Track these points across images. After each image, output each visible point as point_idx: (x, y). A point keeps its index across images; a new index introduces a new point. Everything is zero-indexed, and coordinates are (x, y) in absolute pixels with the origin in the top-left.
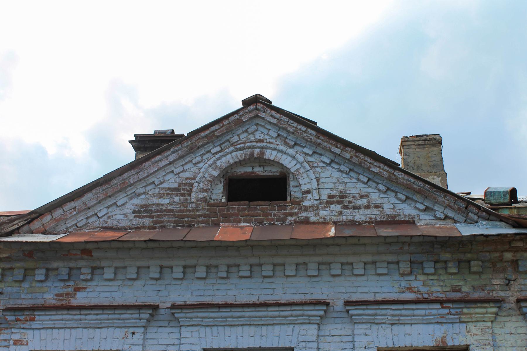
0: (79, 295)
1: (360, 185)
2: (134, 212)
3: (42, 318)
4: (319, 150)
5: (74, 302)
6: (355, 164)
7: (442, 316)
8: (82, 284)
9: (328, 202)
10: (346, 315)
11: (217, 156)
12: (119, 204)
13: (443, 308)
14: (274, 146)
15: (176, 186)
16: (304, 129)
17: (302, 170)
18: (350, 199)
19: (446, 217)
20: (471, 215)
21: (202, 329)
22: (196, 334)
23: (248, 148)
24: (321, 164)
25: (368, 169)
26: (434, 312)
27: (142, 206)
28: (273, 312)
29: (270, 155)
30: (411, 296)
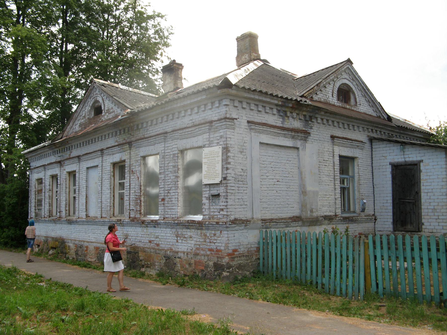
5: (71, 156)
13: (119, 147)
23: (95, 97)
26: (117, 149)
30: (116, 144)
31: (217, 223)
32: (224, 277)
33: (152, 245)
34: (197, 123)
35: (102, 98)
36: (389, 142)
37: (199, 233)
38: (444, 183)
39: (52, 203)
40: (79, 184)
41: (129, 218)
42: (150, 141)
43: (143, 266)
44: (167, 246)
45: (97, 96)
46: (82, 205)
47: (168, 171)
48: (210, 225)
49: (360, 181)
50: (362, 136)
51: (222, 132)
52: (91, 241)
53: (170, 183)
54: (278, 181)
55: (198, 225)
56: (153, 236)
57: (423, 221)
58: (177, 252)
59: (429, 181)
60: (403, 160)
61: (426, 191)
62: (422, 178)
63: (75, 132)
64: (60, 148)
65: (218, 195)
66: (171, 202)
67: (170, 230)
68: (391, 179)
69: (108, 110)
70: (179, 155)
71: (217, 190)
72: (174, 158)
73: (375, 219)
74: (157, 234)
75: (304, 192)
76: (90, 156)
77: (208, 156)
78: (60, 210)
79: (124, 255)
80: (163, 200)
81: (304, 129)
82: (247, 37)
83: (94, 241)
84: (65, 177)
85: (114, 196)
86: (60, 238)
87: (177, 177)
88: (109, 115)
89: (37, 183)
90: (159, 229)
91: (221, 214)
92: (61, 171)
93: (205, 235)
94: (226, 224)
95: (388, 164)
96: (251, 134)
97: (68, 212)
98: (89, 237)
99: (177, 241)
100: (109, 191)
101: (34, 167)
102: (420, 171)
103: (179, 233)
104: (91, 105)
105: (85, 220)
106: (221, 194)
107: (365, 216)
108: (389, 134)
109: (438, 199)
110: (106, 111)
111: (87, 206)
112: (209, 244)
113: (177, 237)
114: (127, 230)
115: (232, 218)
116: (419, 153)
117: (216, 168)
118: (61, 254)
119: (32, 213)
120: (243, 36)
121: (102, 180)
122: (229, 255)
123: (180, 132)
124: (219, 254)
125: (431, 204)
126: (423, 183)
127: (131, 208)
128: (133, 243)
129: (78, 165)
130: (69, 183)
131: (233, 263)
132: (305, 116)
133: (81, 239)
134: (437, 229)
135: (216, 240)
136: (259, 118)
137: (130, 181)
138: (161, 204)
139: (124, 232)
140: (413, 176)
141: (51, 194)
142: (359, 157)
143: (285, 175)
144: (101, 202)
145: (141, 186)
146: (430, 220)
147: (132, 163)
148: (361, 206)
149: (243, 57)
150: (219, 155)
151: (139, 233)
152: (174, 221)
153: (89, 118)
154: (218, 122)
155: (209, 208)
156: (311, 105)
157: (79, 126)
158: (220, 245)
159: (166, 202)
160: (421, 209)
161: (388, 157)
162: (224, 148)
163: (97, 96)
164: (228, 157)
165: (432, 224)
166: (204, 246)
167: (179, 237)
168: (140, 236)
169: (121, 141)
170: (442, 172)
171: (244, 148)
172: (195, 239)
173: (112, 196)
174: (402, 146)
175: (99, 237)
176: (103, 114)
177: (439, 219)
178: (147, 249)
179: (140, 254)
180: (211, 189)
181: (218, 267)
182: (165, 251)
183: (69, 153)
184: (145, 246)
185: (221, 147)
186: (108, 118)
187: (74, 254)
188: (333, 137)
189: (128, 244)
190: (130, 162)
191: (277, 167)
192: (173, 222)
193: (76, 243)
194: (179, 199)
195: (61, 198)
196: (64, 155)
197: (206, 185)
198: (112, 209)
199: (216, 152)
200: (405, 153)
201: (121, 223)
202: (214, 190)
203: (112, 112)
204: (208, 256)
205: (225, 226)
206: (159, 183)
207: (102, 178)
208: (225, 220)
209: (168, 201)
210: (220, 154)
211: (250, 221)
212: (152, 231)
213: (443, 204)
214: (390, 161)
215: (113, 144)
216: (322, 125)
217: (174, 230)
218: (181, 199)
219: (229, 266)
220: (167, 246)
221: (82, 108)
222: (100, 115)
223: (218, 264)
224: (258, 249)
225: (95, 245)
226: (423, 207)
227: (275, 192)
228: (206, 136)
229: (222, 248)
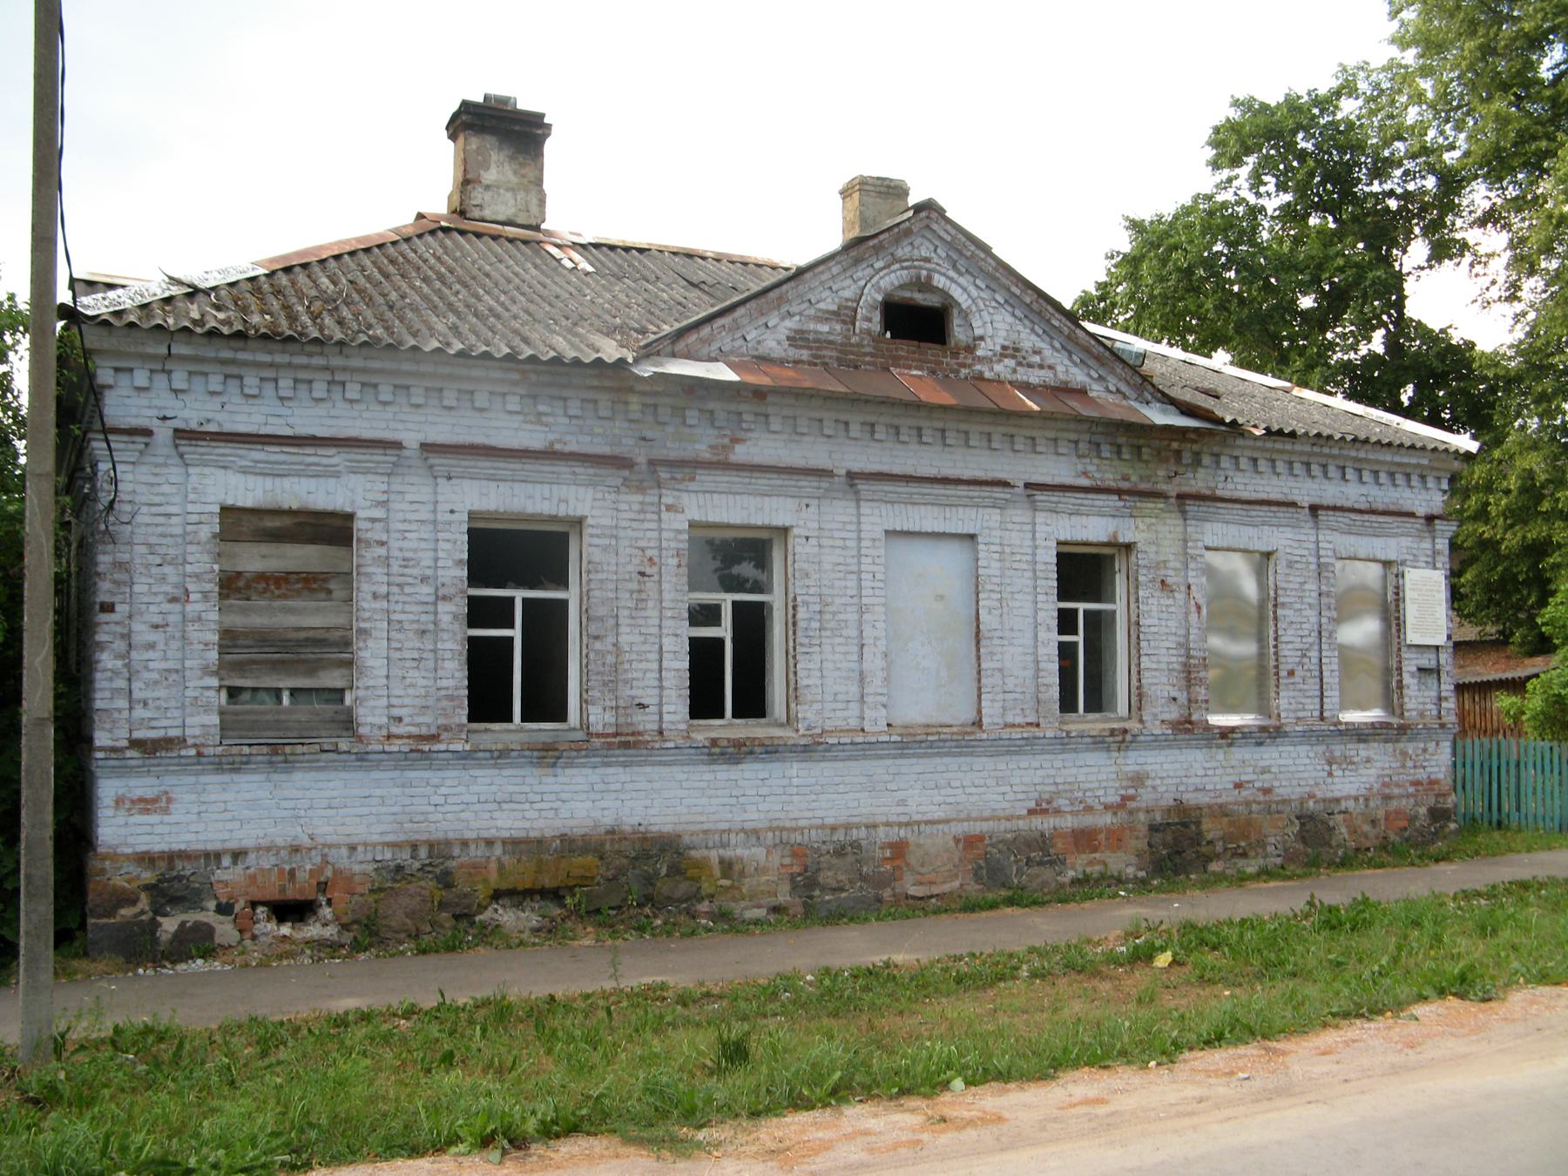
0: (739, 448)
1: (1033, 337)
2: (788, 338)
3: (703, 478)
4: (993, 285)
5: (733, 458)
6: (1032, 310)
7: (1117, 509)
8: (741, 435)
9: (1001, 355)
10: (1025, 499)
11: (881, 274)
12: (770, 325)
13: (1120, 499)
14: (943, 271)
15: (835, 308)
16: (983, 256)
17: (974, 309)
18: (1024, 353)
19: (1118, 391)
20: (1146, 394)
21: (883, 506)
22: (876, 512)
23: (915, 267)
24: (994, 304)
25: (1048, 321)
26: (1111, 503)
27: (796, 331)
28: (962, 491)
29: (939, 281)
30: (1085, 482)
32: (1451, 832)
33: (1245, 793)
34: (1381, 507)
42: (1254, 513)
47: (1302, 603)
56: (1251, 769)
58: (1337, 800)
74: (1261, 763)
79: (1137, 838)
80: (1291, 673)
83: (939, 814)
86: (612, 832)
90: (1274, 748)
93: (1404, 754)
98: (902, 802)
99: (1330, 774)
103: (1337, 754)
113: (1330, 763)
114: (1141, 760)
117: (1438, 616)
123: (1353, 516)
139: (1128, 768)
151: (1196, 765)
158: (1436, 769)
168: (1200, 772)
169: (1110, 478)
172: (1378, 765)
175: (972, 799)
179: (1206, 825)
181: (1439, 815)
187: (786, 887)
212: (1247, 756)
215: (1069, 480)
217: (1321, 749)
220: (1299, 790)
225: (959, 829)
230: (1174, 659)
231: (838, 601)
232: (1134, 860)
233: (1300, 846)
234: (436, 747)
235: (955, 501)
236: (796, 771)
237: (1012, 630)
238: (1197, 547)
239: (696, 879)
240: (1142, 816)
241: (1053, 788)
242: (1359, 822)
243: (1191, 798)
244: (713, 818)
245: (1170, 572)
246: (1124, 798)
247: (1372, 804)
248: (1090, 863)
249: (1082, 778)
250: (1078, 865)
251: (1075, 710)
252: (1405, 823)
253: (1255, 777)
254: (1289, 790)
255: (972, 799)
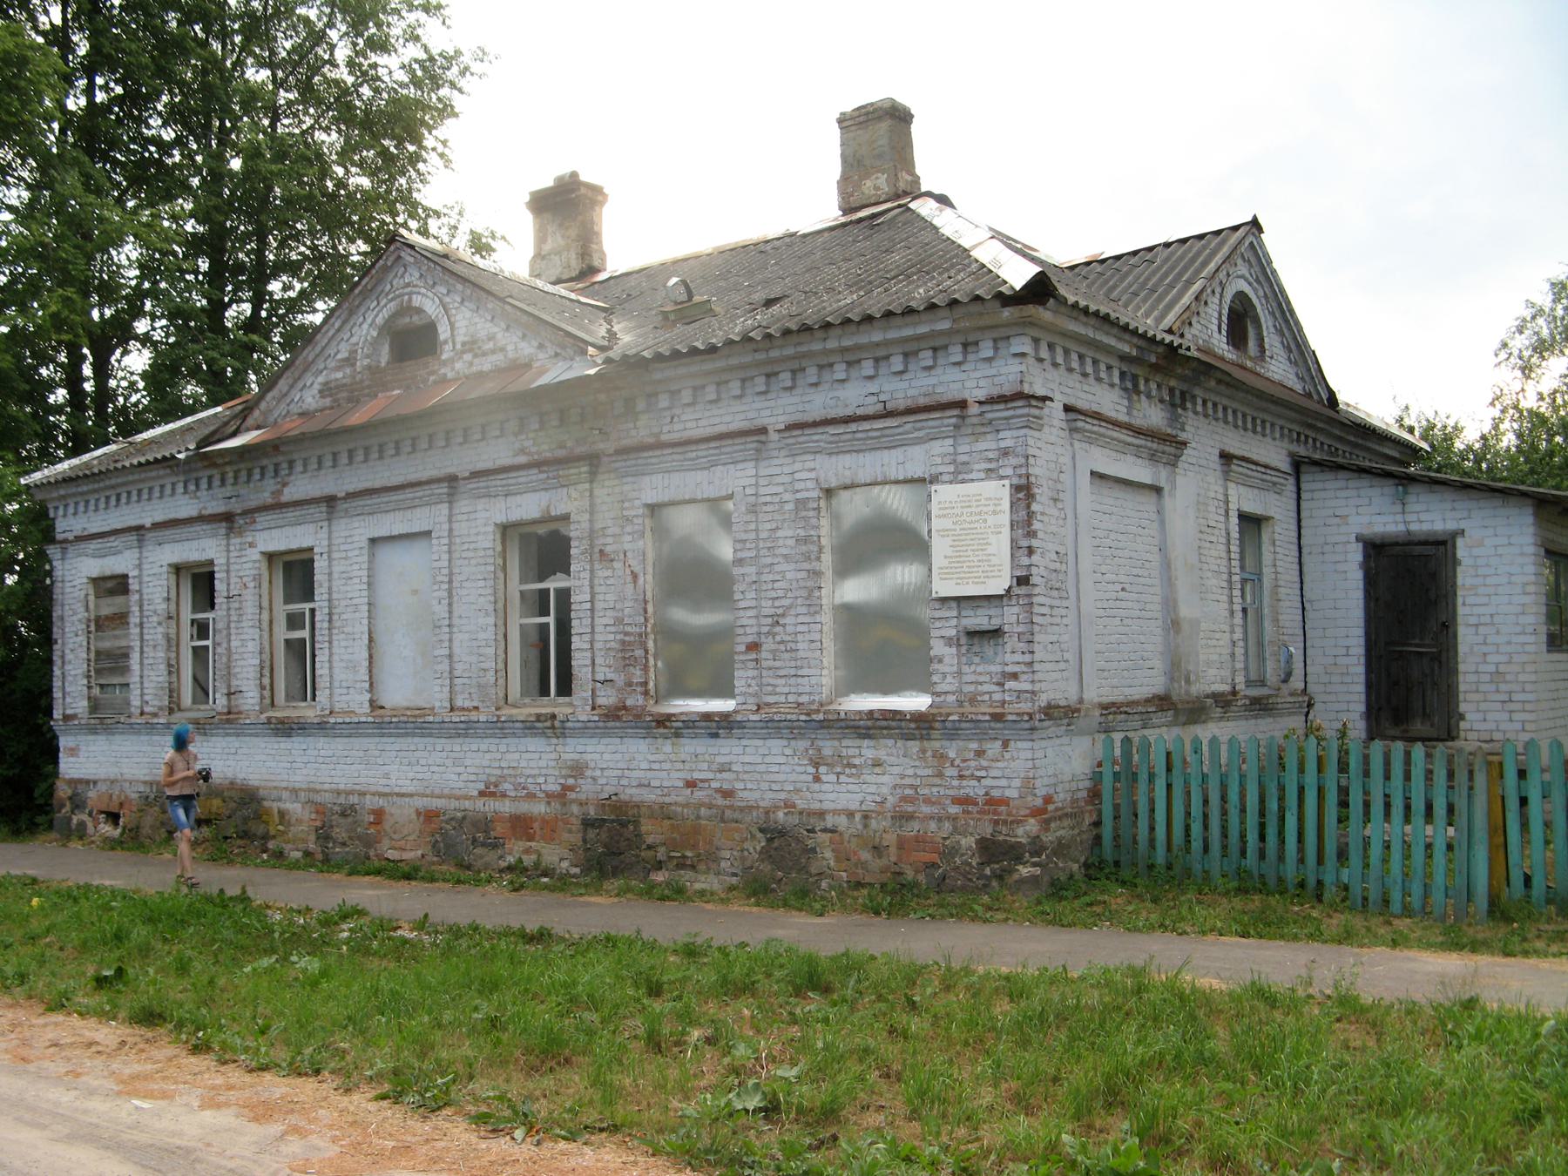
0: (286, 490)
13: (541, 472)
23: (398, 296)
26: (534, 478)
30: (522, 459)
31: (998, 717)
33: (699, 794)
34: (902, 404)
35: (441, 301)
36: (1356, 475)
37: (915, 750)
38: (1527, 599)
39: (178, 663)
40: (330, 594)
41: (593, 708)
43: (659, 865)
44: (771, 795)
45: (410, 294)
46: (354, 668)
47: (775, 555)
48: (964, 725)
49: (1280, 589)
50: (1274, 453)
51: (1008, 439)
52: (397, 790)
53: (780, 593)
54: (1123, 589)
55: (913, 725)
56: (705, 766)
57: (1463, 707)
58: (821, 814)
59: (1481, 590)
60: (1401, 528)
61: (1473, 620)
62: (1460, 581)
63: (301, 415)
64: (228, 469)
65: (996, 633)
66: (787, 655)
67: (785, 742)
68: (1361, 585)
69: (474, 342)
70: (823, 503)
71: (990, 617)
72: (804, 514)
73: (1310, 705)
75: (1174, 625)
76: (394, 498)
77: (958, 511)
78: (229, 686)
79: (570, 831)
80: (754, 647)
81: (1169, 431)
82: (880, 118)
83: (411, 789)
84: (256, 572)
85: (505, 636)
86: (232, 783)
87: (817, 574)
88: (476, 361)
89: (91, 592)
90: (735, 742)
91: (1010, 690)
92: (228, 551)
93: (941, 757)
94: (1031, 718)
95: (1353, 538)
96: (1072, 445)
97: (267, 693)
98: (387, 776)
99: (817, 779)
100: (491, 620)
101: (75, 533)
102: (1455, 562)
103: (827, 752)
104: (379, 321)
105: (370, 719)
106: (1006, 628)
107: (1291, 694)
108: (1329, 446)
109: (1509, 643)
110: (459, 346)
111: (374, 671)
112: (955, 783)
113: (816, 765)
114: (579, 748)
115: (1043, 700)
116: (1454, 509)
118: (240, 842)
119: (68, 700)
120: (867, 114)
121: (450, 582)
122: (1036, 812)
124: (995, 812)
125: (1490, 658)
126: (1464, 596)
127: (600, 677)
128: (609, 790)
129: (325, 530)
130: (270, 594)
131: (1048, 838)
132: (1172, 391)
133: (342, 787)
134: (1504, 732)
135: (986, 769)
136: (1084, 396)
137: (592, 587)
138: (743, 662)
140: (1433, 576)
141: (173, 631)
142: (1277, 517)
143: (1135, 571)
144: (450, 656)
145: (646, 602)
146: (1483, 706)
147: (598, 525)
148: (1282, 664)
149: (869, 183)
150: (998, 508)
151: (639, 757)
152: (808, 714)
153: (369, 367)
154: (1002, 406)
155: (960, 673)
156: (1198, 359)
157: (320, 392)
158: (1003, 782)
159: (764, 655)
160: (1456, 671)
161: (1351, 520)
162: (1017, 489)
163: (410, 294)
164: (1031, 515)
165: (1490, 716)
166: (935, 790)
167: (827, 765)
168: (644, 765)
169: (546, 449)
170: (1522, 566)
171: (1059, 487)
173: (500, 637)
174: (1400, 488)
175: (436, 777)
176: (444, 357)
177: (1511, 701)
178: (679, 809)
179: (646, 826)
180: (963, 613)
182: (767, 813)
183: (274, 488)
184: (667, 800)
185: (1007, 482)
186: (474, 369)
187: (313, 837)
188: (1226, 457)
189: (583, 797)
190: (591, 521)
191: (1120, 545)
192: (803, 718)
193: (318, 798)
194: (825, 645)
195: (233, 644)
196: (242, 492)
197: (944, 600)
198: (501, 681)
199: (986, 499)
200: (1408, 508)
201: (553, 727)
202: (976, 616)
203: (493, 352)
204: (955, 819)
205: (1027, 725)
206: (734, 592)
207: (451, 574)
208: (1025, 707)
209: (773, 652)
210: (1006, 505)
211: (1078, 710)
212: (700, 750)
213: (1525, 658)
214: (1356, 529)
216: (1201, 418)
217: (802, 744)
218: (829, 644)
219: (1036, 847)
220: (771, 795)
221: (338, 330)
222: (430, 359)
223: (994, 842)
224: (1095, 794)
225: (420, 803)
226: (1462, 667)
227: (1117, 621)
228: (942, 447)
229: (1012, 793)
230: (611, 637)
231: (343, 603)
232: (566, 853)
233: (766, 867)
234: (155, 721)
235: (417, 502)
236: (322, 746)
237: (460, 617)
238: (633, 508)
239: (267, 823)
240: (575, 809)
241: (498, 772)
242: (853, 845)
243: (631, 793)
244: (279, 778)
245: (609, 540)
246: (565, 788)
247: (873, 824)
248: (527, 851)
249: (523, 764)
250: (515, 851)
251: (548, 695)
252: (935, 858)
253: (711, 775)
254: (757, 795)
255: (436, 777)
